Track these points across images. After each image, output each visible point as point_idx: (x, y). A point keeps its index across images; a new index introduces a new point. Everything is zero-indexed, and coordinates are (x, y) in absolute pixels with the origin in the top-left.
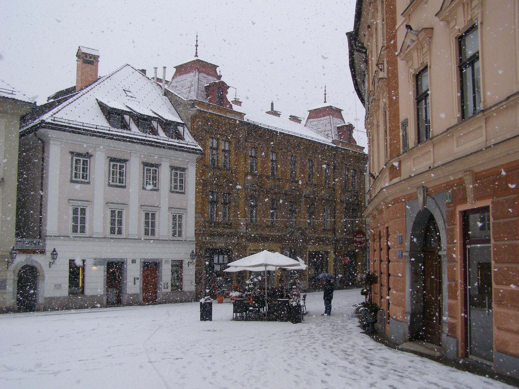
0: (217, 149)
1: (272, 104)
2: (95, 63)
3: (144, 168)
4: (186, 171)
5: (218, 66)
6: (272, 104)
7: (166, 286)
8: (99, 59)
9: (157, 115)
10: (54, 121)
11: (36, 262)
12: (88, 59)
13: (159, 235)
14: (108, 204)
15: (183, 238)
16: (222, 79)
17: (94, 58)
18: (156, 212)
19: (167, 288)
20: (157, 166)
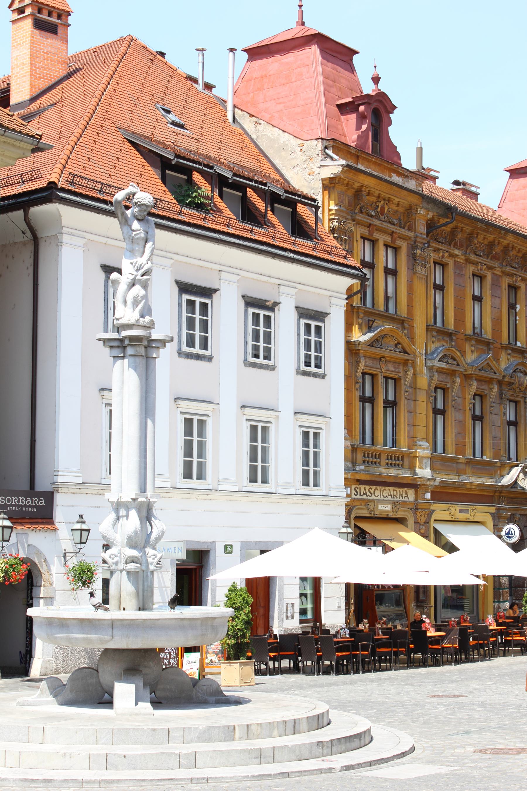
0: (371, 266)
1: (420, 151)
2: (60, 30)
3: (246, 311)
4: (326, 320)
5: (356, 52)
6: (420, 151)
7: (289, 615)
8: (71, 20)
9: (282, 175)
10: (72, 183)
11: (39, 553)
12: (44, 16)
13: (277, 484)
14: (180, 402)
15: (322, 490)
16: (382, 86)
17: (59, 17)
18: (270, 422)
19: (293, 618)
20: (272, 307)
